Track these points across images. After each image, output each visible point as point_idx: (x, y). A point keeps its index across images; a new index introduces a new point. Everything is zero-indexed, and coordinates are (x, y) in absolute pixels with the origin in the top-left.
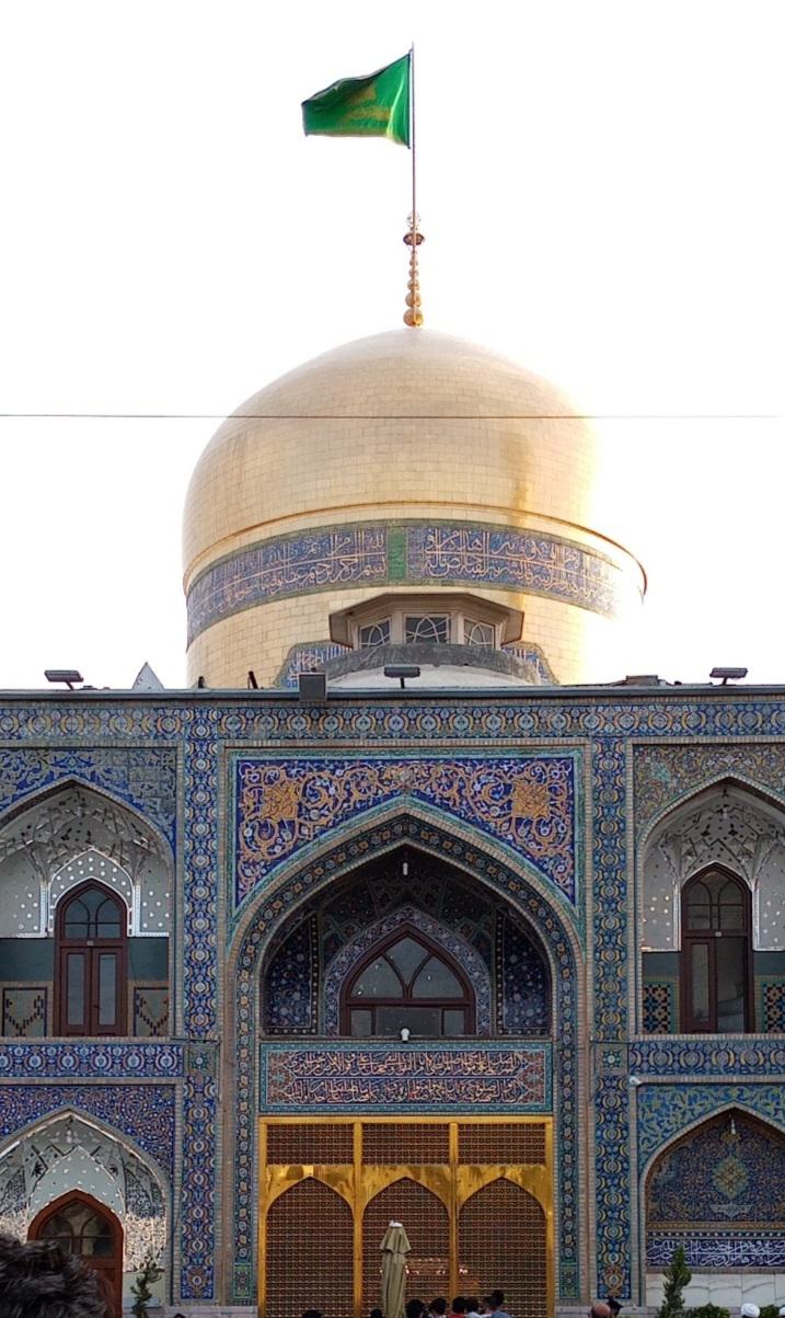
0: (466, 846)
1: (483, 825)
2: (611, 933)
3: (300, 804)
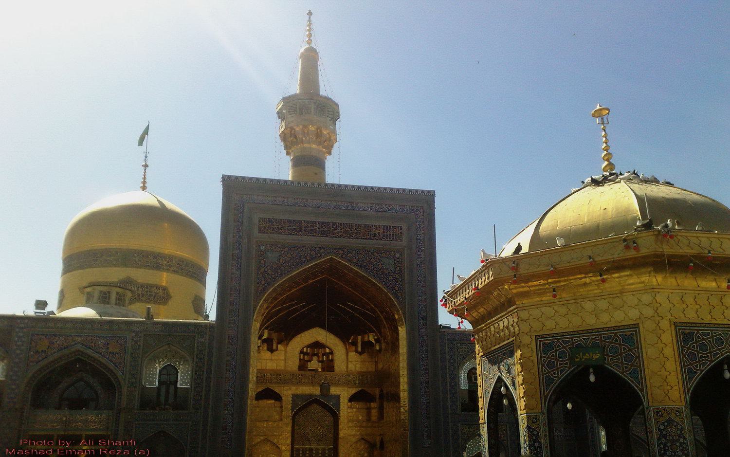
3: (49, 346)
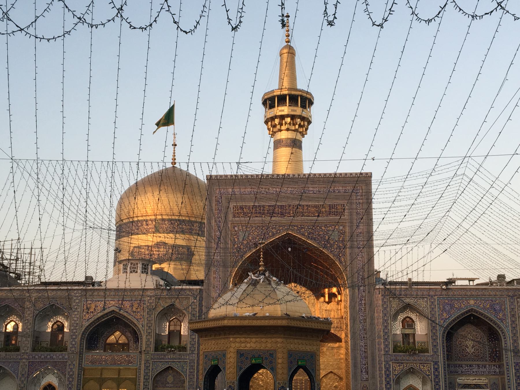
0: (125, 316)
1: (127, 312)
2: (149, 333)
